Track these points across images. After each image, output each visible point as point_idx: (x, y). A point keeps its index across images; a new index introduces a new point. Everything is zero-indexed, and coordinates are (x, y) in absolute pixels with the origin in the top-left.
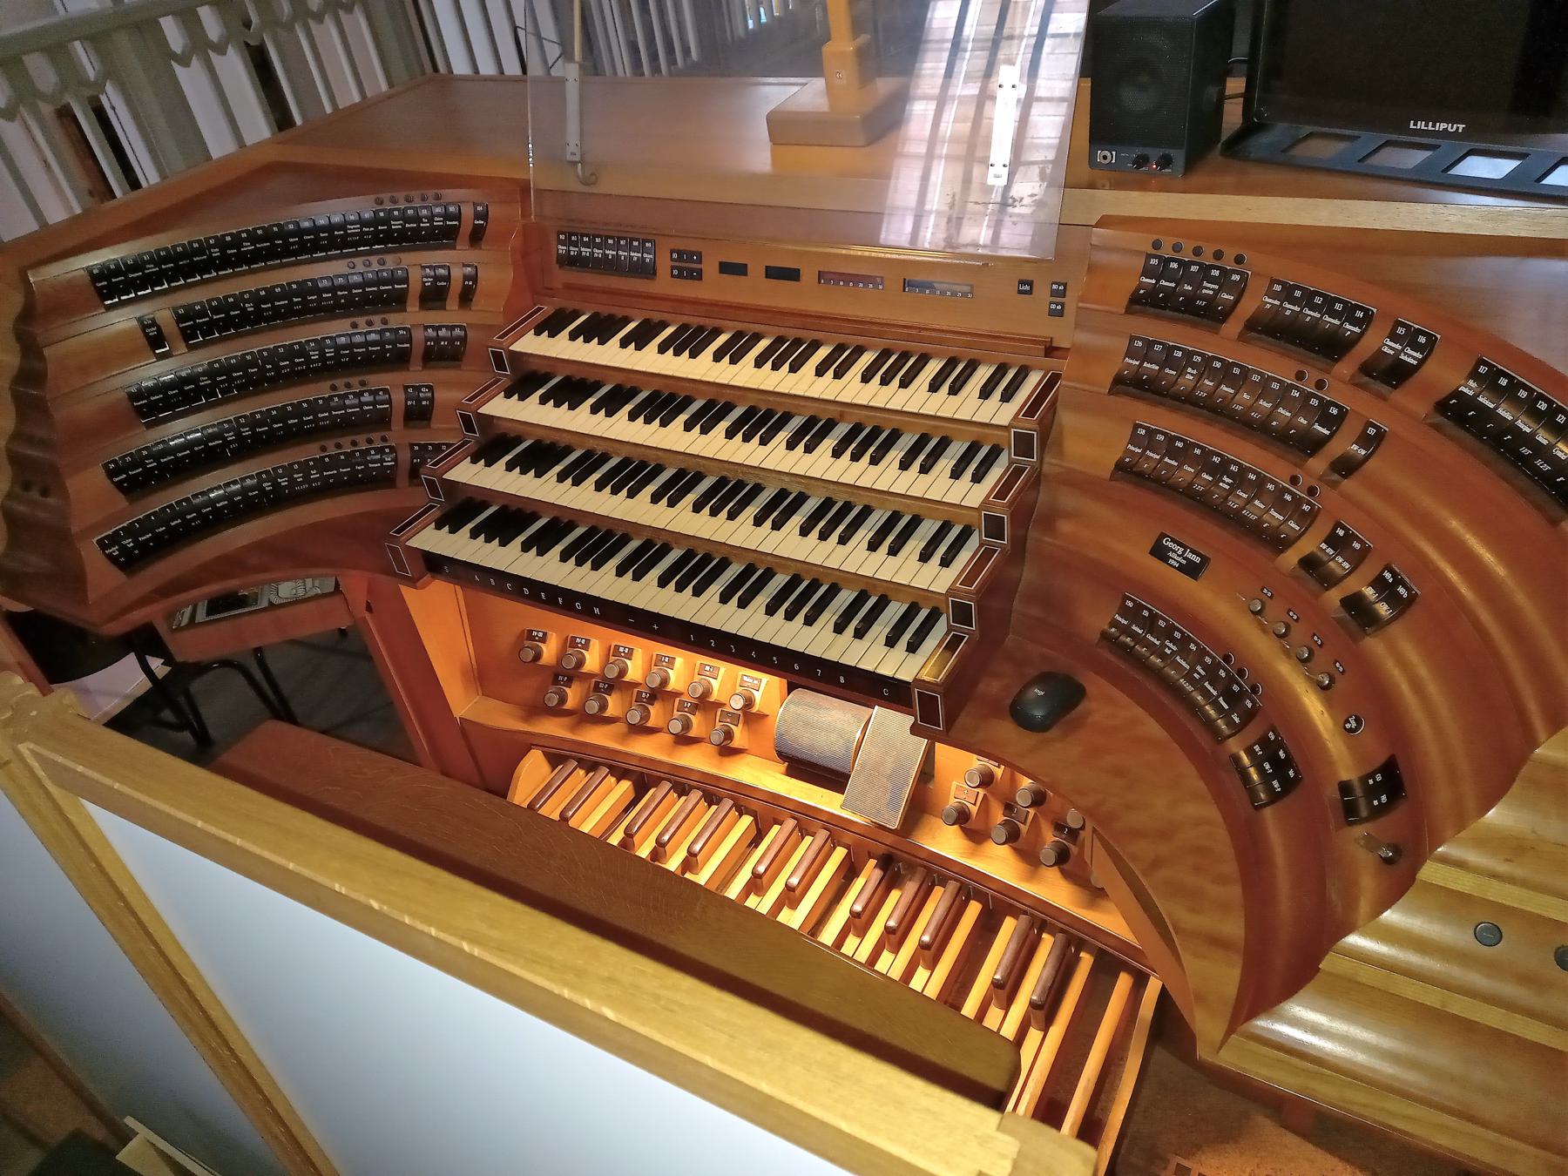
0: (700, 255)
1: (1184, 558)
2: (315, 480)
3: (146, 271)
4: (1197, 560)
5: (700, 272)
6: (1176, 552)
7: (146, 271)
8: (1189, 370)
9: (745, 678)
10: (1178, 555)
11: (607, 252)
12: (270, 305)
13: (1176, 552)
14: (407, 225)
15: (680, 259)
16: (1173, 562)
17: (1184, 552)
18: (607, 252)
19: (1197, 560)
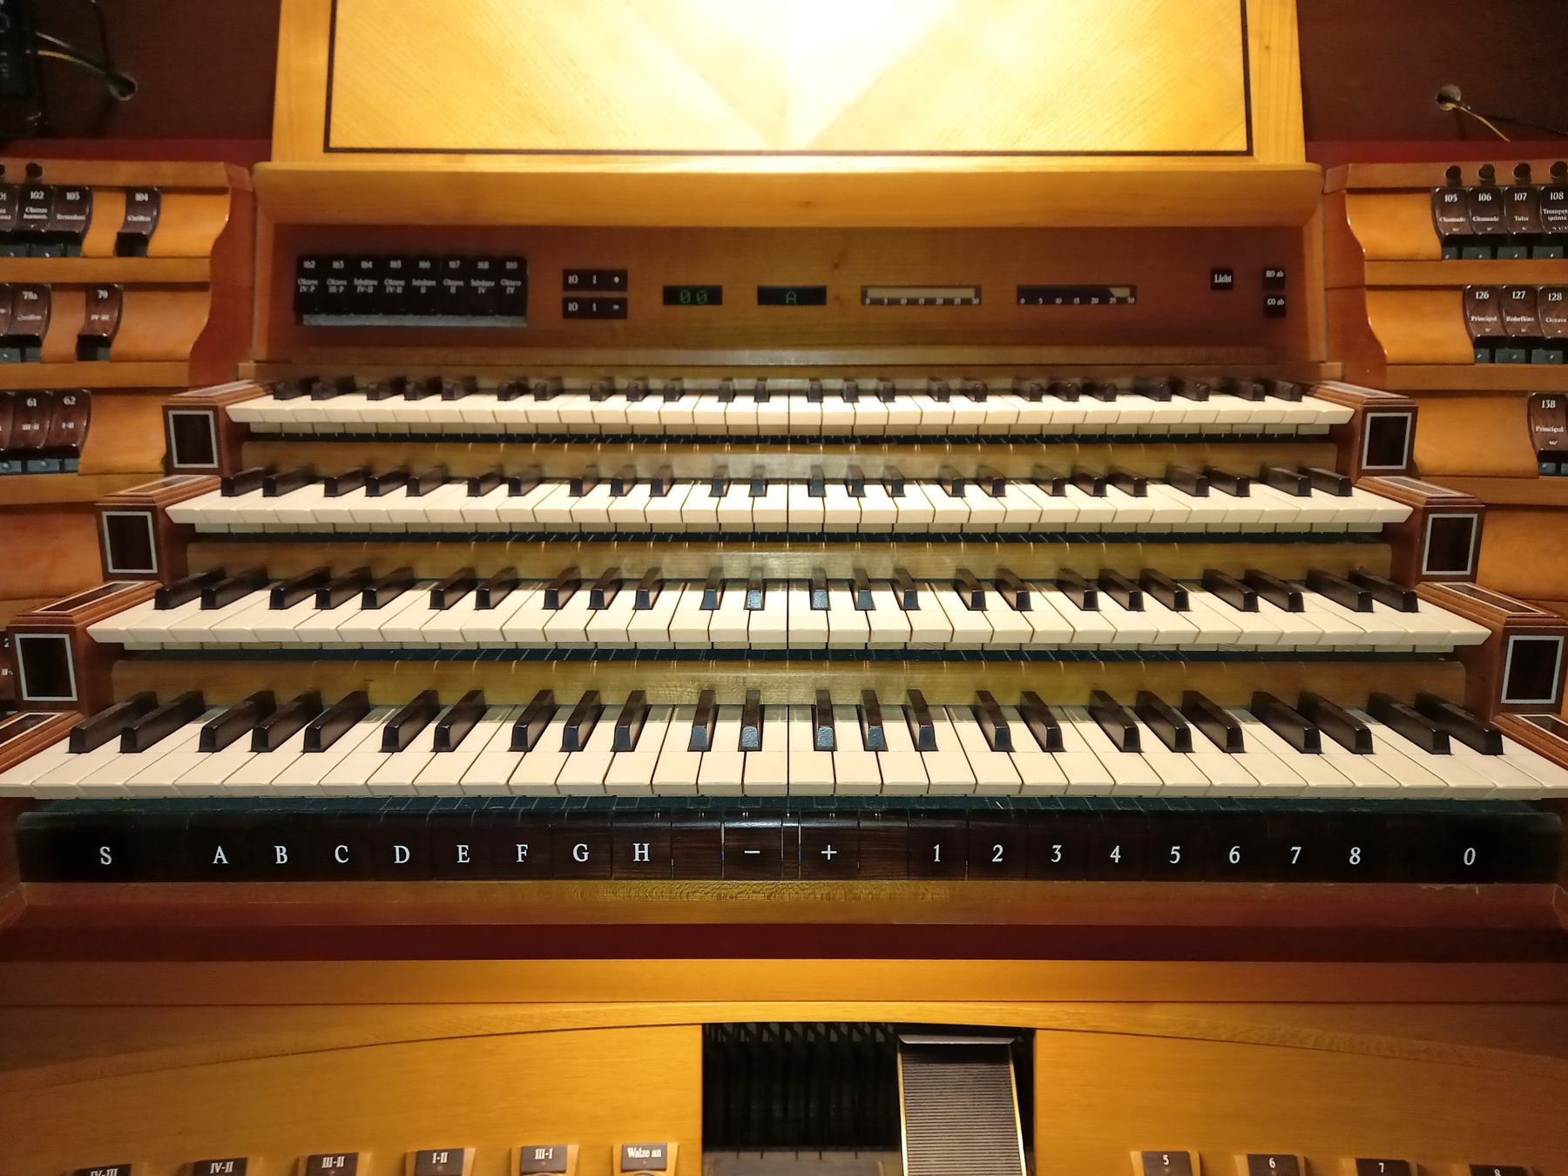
0: (623, 275)
5: (623, 302)
9: (632, 1153)
11: (416, 283)
15: (585, 282)
18: (416, 283)
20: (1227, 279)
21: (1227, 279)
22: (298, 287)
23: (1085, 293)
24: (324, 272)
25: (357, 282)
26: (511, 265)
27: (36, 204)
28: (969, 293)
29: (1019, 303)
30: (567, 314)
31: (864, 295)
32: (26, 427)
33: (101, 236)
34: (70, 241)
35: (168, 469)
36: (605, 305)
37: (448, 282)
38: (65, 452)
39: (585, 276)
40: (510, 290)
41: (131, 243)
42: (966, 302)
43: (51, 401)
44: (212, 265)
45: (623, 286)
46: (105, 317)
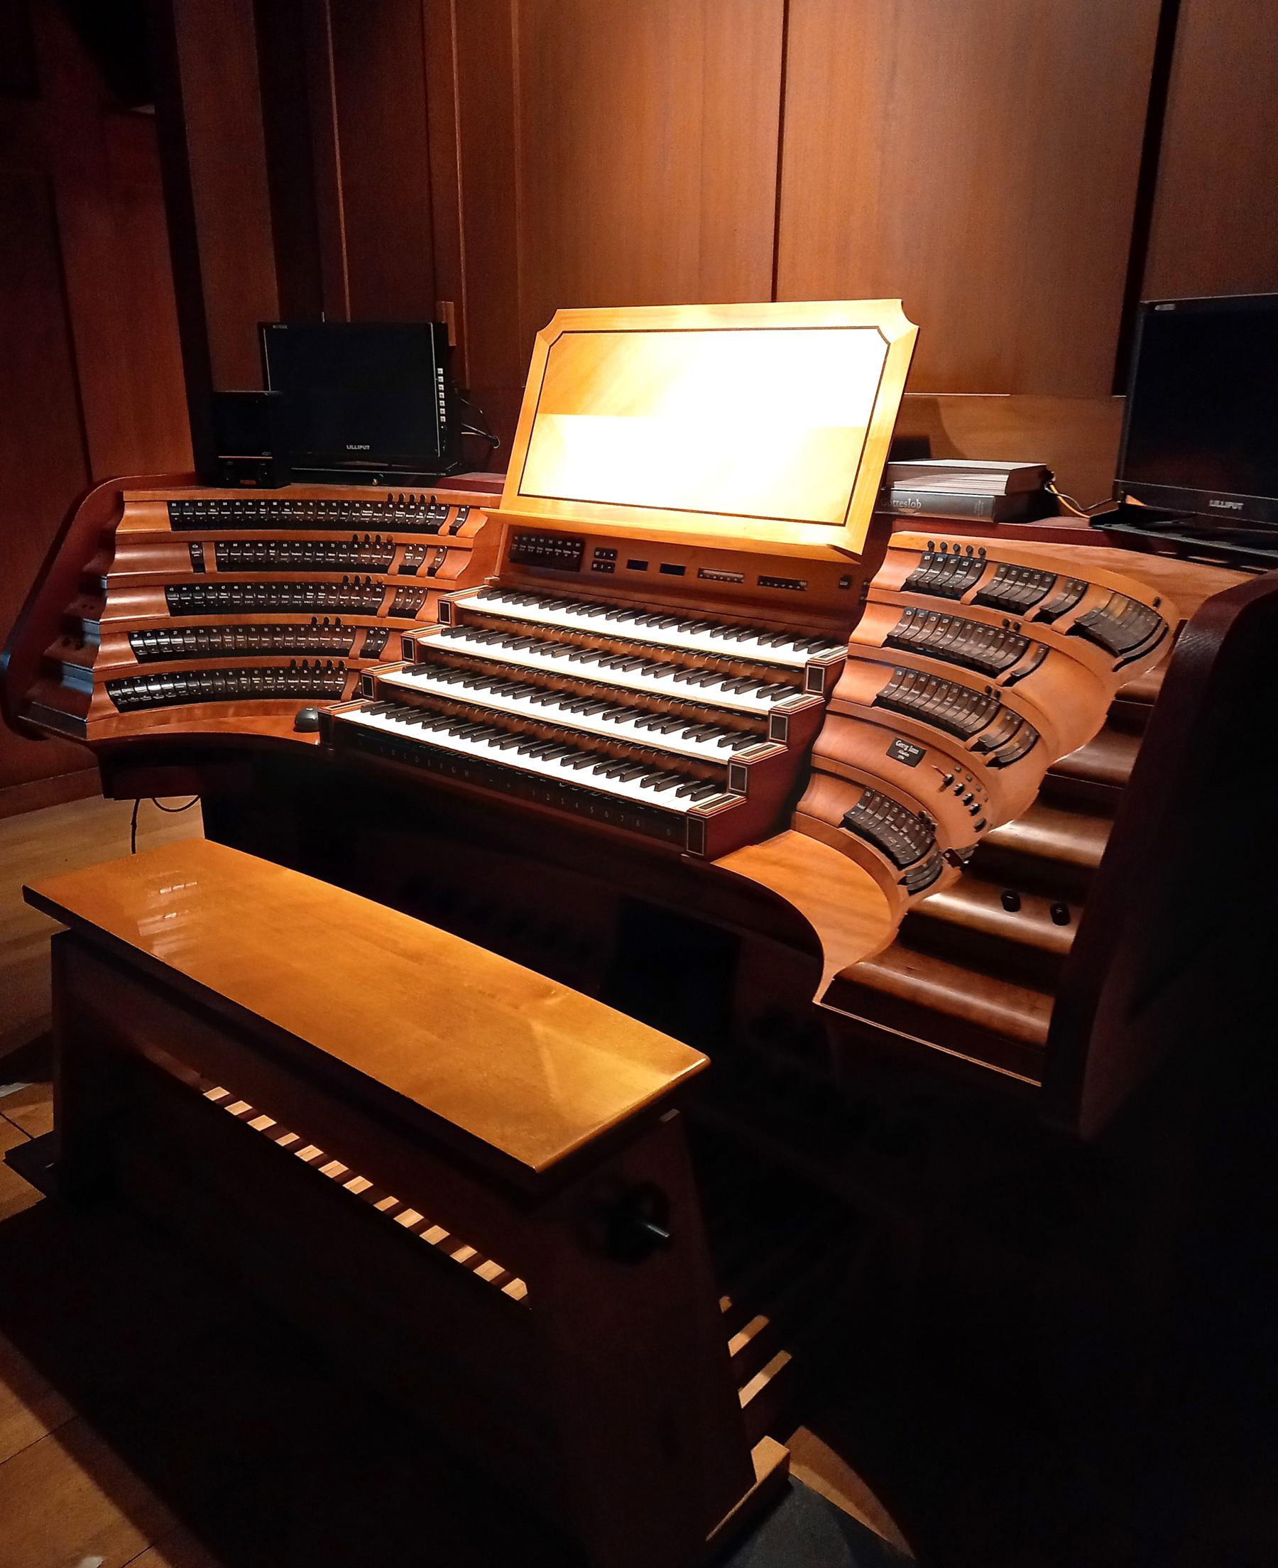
0: (615, 552)
1: (909, 753)
2: (281, 684)
3: (209, 513)
4: (916, 752)
5: (613, 565)
6: (903, 749)
7: (209, 513)
8: (940, 629)
10: (905, 751)
11: (546, 549)
12: (287, 554)
13: (903, 749)
14: (407, 516)
16: (900, 757)
17: (908, 749)
19: (916, 752)
20: (846, 584)
21: (846, 584)
22: (511, 547)
23: (788, 582)
24: (520, 542)
25: (529, 547)
26: (578, 545)
27: (432, 511)
28: (742, 576)
29: (759, 584)
30: (593, 569)
31: (701, 571)
32: (407, 600)
33: (445, 528)
34: (433, 529)
35: (439, 623)
36: (606, 564)
37: (557, 550)
38: (412, 614)
39: (602, 550)
40: (575, 556)
41: (453, 531)
42: (739, 581)
43: (415, 592)
44: (474, 541)
45: (614, 558)
46: (439, 560)
